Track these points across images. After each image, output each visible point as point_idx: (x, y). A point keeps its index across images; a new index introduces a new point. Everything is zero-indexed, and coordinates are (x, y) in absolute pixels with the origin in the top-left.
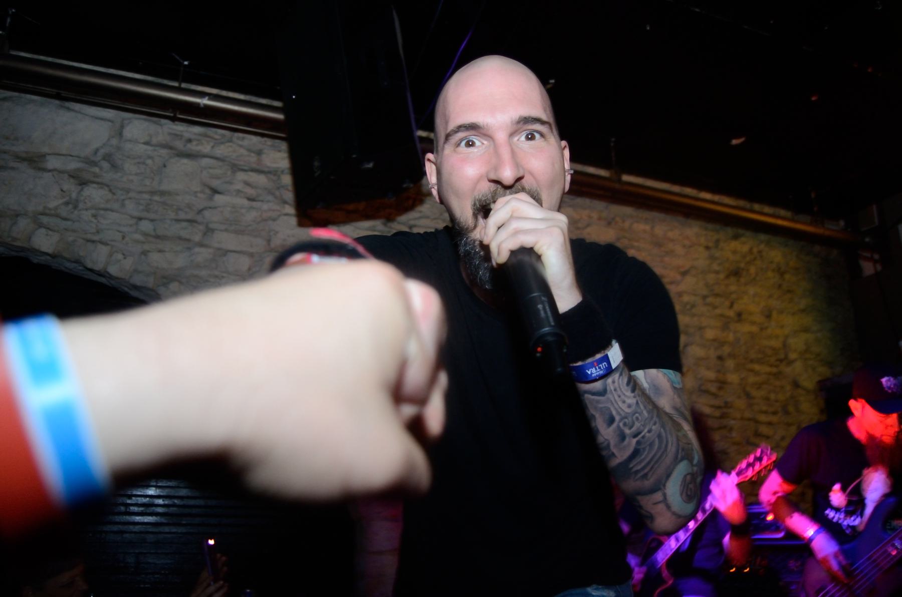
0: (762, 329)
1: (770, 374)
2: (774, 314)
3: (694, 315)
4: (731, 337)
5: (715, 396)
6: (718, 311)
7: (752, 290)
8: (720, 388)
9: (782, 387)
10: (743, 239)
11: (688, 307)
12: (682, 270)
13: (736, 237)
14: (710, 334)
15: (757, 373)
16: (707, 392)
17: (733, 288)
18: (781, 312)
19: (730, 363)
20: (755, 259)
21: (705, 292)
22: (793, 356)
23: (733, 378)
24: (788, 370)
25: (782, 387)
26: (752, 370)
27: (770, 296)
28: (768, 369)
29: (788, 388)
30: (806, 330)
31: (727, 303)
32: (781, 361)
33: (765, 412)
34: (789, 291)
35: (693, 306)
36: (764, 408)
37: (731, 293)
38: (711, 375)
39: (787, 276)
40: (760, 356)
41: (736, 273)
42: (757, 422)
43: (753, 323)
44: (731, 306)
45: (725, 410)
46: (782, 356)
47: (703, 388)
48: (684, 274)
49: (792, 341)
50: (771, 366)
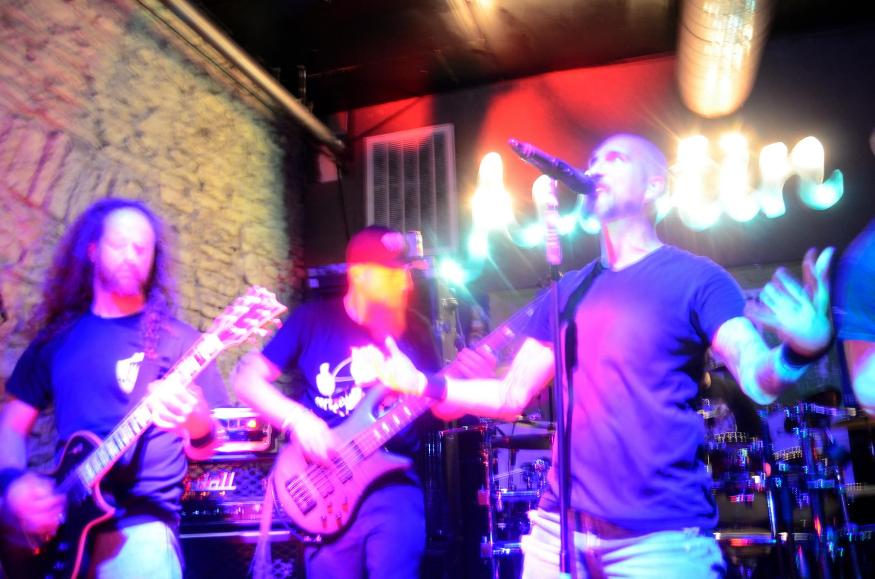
1: (223, 262)
2: (236, 198)
3: (154, 166)
4: (189, 208)
7: (219, 160)
10: (219, 98)
11: (149, 153)
12: (151, 105)
13: (214, 93)
17: (200, 150)
18: (241, 195)
22: (246, 247)
24: (239, 262)
25: (232, 279)
27: (234, 174)
28: (224, 257)
29: (238, 282)
30: (261, 222)
31: (192, 165)
32: (235, 249)
33: (213, 306)
34: (252, 176)
35: (155, 155)
36: (213, 300)
39: (253, 158)
40: (216, 238)
42: (202, 315)
43: (214, 198)
44: (195, 171)
46: (235, 245)
48: (151, 110)
50: (225, 253)
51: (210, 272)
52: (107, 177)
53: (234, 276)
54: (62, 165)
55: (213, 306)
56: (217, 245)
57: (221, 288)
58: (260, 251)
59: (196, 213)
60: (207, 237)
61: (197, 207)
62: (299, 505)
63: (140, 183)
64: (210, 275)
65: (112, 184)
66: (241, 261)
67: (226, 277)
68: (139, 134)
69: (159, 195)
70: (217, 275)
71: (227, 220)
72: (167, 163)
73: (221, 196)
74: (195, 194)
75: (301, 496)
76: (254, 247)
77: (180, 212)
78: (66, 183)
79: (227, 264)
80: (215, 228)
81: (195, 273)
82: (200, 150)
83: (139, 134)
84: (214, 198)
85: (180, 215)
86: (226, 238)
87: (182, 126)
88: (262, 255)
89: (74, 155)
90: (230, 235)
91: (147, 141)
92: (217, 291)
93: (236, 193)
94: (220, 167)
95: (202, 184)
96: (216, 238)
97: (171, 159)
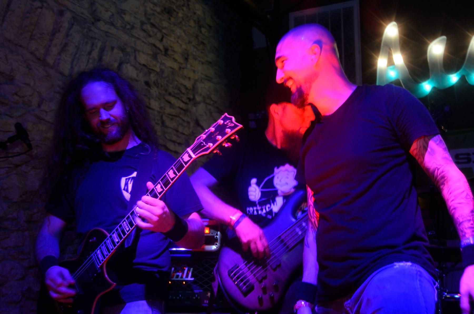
0: (180, 68)
1: (181, 109)
2: (191, 60)
3: (132, 36)
6: (152, 40)
7: (178, 32)
9: (188, 123)
11: (128, 27)
14: (143, 59)
17: (165, 24)
20: (183, 6)
21: (144, 19)
22: (198, 98)
25: (188, 123)
26: (169, 102)
27: (190, 42)
28: (182, 105)
29: (192, 124)
31: (159, 35)
33: (174, 142)
34: (203, 43)
35: (133, 27)
36: (174, 138)
37: (163, 28)
39: (203, 30)
40: (176, 91)
41: (168, 11)
43: (175, 60)
44: (161, 40)
46: (192, 97)
49: (199, 85)
50: (183, 102)
51: (173, 117)
52: (99, 44)
53: (189, 120)
54: (67, 36)
55: (174, 142)
56: (178, 96)
57: (180, 129)
58: (208, 101)
59: (162, 71)
60: (171, 90)
61: (163, 68)
62: (240, 288)
63: (122, 50)
64: (172, 119)
65: (102, 51)
66: (194, 108)
67: (183, 120)
68: (122, 12)
69: (135, 58)
70: (178, 119)
71: (185, 77)
72: (142, 34)
73: (181, 60)
74: (161, 58)
75: (242, 280)
76: (204, 97)
77: (150, 71)
78: (71, 49)
79: (184, 110)
80: (176, 83)
81: (162, 118)
82: (165, 24)
83: (122, 12)
84: (175, 60)
85: (150, 73)
86: (184, 90)
87: (151, 6)
88: (209, 104)
89: (76, 27)
90: (186, 88)
91: (127, 18)
92: (177, 131)
93: (190, 57)
94: (179, 37)
95: (166, 50)
96: (176, 91)
97: (144, 31)
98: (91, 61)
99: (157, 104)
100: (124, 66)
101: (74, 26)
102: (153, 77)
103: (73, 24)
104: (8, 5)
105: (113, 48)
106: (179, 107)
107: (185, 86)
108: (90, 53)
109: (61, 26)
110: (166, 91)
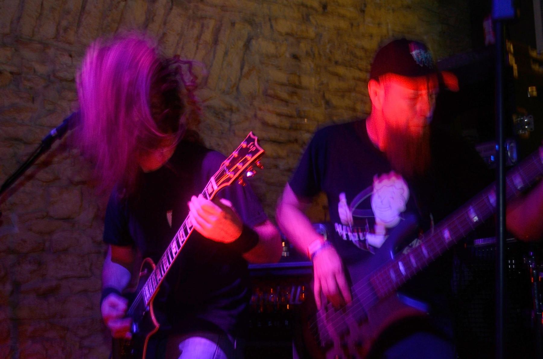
0: (352, 25)
5: (286, 102)
8: (293, 94)
14: (283, 26)
15: (340, 77)
16: (276, 97)
19: (307, 64)
23: (310, 81)
26: (336, 75)
38: (282, 77)
43: (343, 17)
45: (298, 120)
47: (270, 92)
51: (343, 93)
54: (165, 23)
59: (319, 35)
63: (250, 21)
64: (343, 96)
81: (324, 96)
84: (343, 17)
86: (360, 53)
89: (176, 10)
98: (200, 46)
99: (313, 80)
100: (254, 42)
101: (173, 11)
102: (304, 47)
103: (171, 9)
104: (83, 7)
105: (233, 24)
106: (354, 78)
107: (363, 48)
108: (199, 38)
109: (155, 15)
110: (330, 60)
